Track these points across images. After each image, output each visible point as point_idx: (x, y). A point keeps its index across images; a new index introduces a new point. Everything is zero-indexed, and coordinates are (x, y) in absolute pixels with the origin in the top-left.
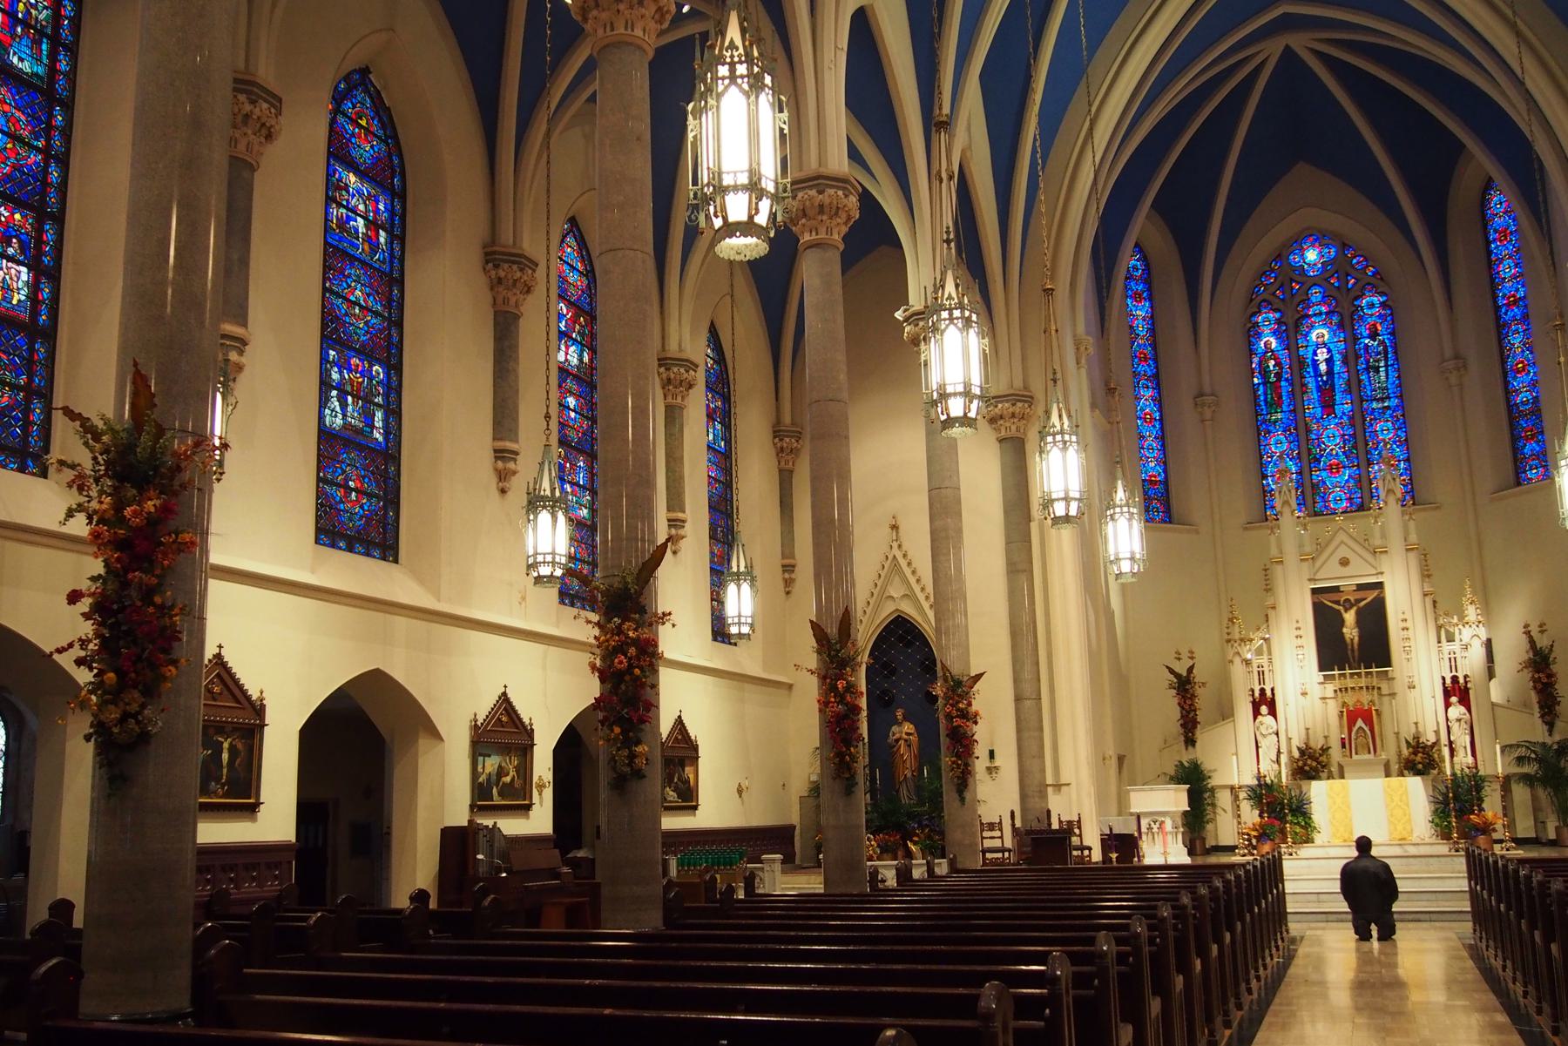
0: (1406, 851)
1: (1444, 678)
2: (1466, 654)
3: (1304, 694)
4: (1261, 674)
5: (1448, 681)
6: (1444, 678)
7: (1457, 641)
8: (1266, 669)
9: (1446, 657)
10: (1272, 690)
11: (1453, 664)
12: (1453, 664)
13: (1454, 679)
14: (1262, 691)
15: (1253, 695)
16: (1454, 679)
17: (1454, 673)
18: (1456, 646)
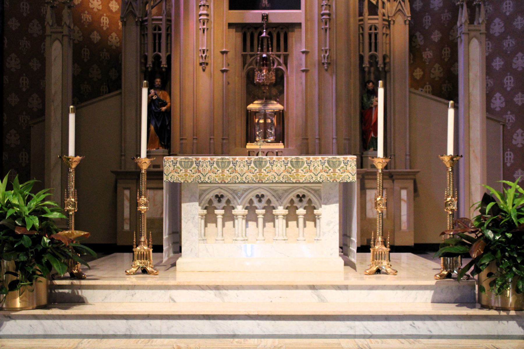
0: (322, 300)
1: (361, 58)
2: (388, 32)
3: (204, 64)
4: (157, 38)
5: (366, 60)
6: (361, 58)
7: (380, 16)
8: (163, 32)
9: (367, 31)
10: (169, 59)
11: (373, 40)
12: (373, 40)
13: (373, 57)
14: (157, 58)
15: (146, 63)
16: (373, 57)
17: (373, 52)
18: (377, 21)
